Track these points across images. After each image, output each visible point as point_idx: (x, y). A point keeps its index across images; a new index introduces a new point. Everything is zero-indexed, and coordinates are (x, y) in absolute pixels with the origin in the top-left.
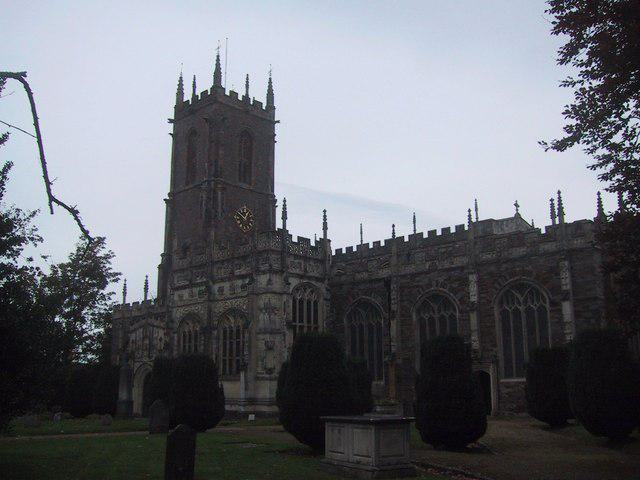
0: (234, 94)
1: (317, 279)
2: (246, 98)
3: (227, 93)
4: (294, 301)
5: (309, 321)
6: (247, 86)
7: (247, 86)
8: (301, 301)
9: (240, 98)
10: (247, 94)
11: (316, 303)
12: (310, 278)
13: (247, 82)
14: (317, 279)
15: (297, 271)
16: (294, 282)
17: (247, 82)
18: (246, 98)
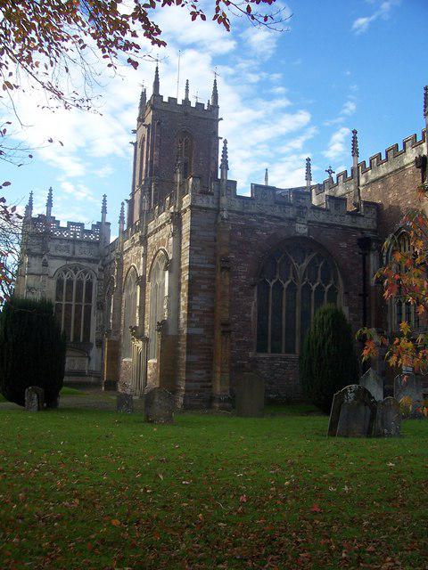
0: (172, 100)
1: (89, 260)
2: (186, 101)
3: (165, 100)
4: (60, 282)
5: (79, 299)
6: (187, 90)
7: (187, 90)
8: (70, 282)
9: (180, 102)
10: (187, 98)
11: (89, 285)
12: (79, 259)
13: (187, 87)
14: (89, 260)
15: (64, 254)
16: (56, 265)
17: (187, 87)
18: (186, 101)
